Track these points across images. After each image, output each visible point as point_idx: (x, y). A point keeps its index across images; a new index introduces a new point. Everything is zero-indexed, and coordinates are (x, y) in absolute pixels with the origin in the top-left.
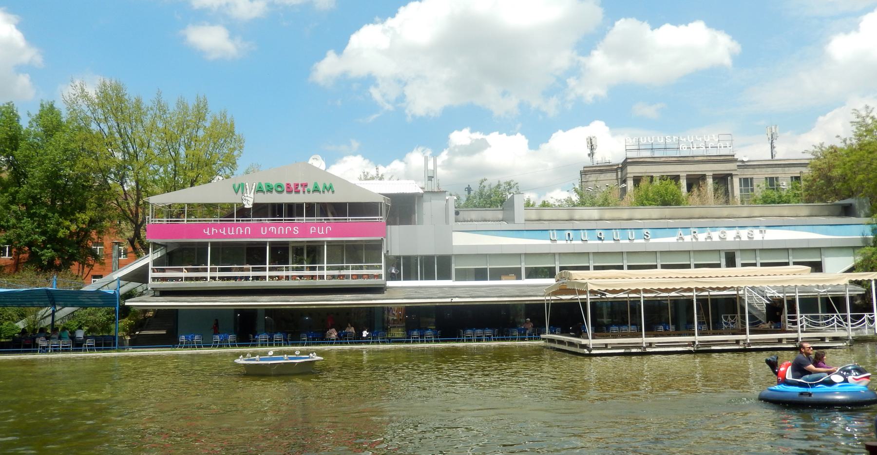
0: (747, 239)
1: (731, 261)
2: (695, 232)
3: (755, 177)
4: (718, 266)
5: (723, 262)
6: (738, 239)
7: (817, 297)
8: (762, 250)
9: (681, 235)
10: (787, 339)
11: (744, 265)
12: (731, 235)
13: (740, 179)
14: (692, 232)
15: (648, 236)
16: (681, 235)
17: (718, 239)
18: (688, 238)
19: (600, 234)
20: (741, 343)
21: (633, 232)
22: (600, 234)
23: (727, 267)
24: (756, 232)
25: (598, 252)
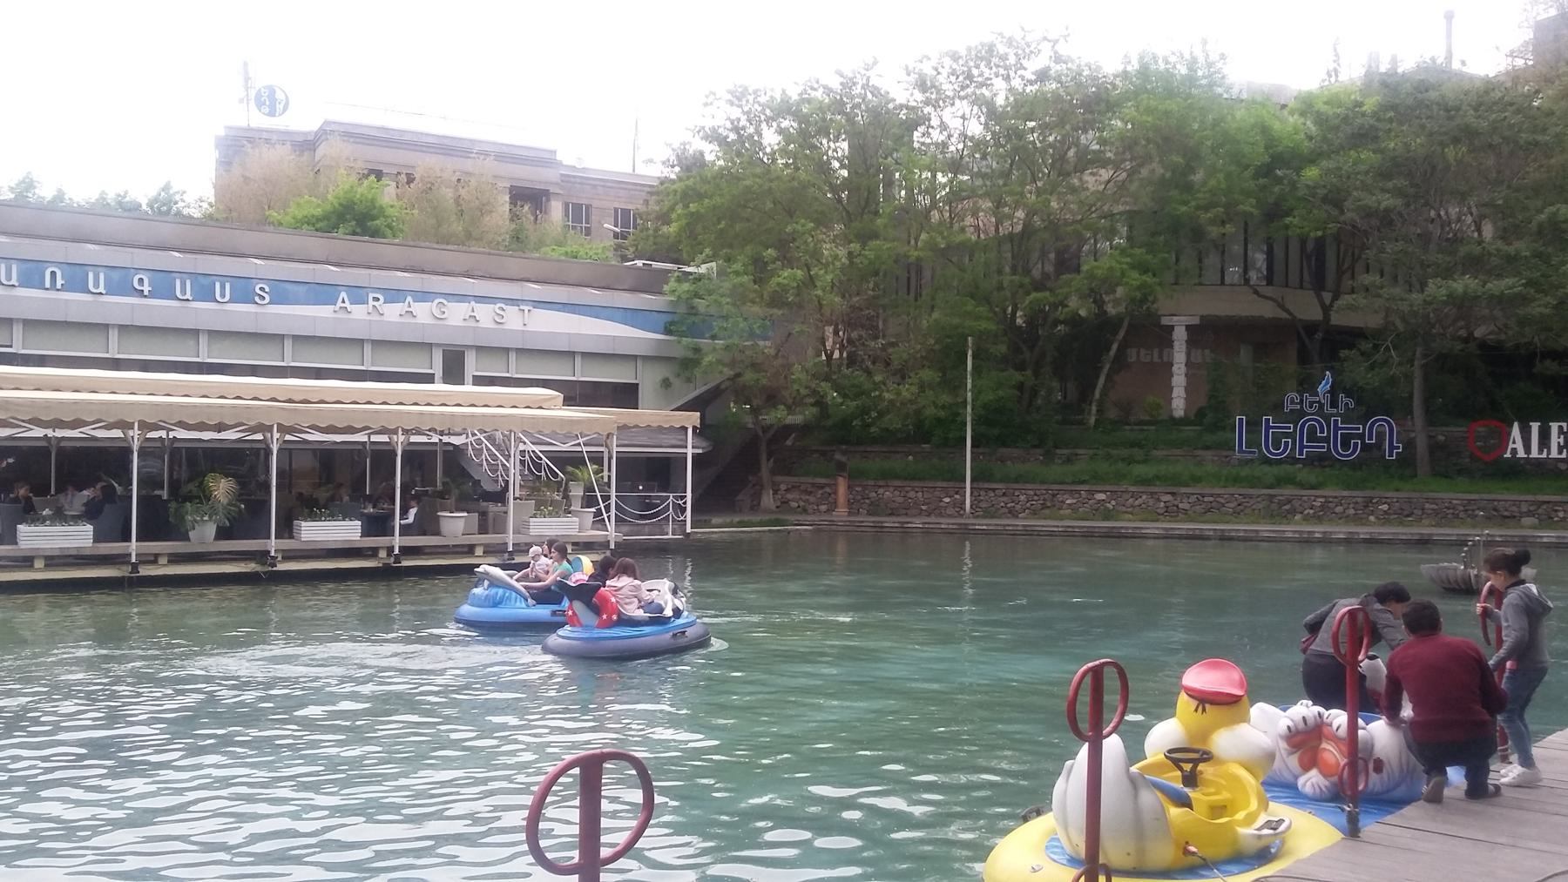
0: (494, 326)
1: (454, 370)
2: (378, 299)
3: (595, 203)
4: (429, 379)
5: (438, 370)
6: (472, 324)
7: (600, 455)
8: (520, 351)
9: (343, 302)
10: (486, 546)
11: (479, 381)
12: (457, 314)
13: (567, 205)
14: (371, 296)
15: (264, 298)
16: (343, 302)
17: (429, 321)
18: (358, 311)
19: (141, 280)
20: (383, 554)
21: (228, 286)
22: (141, 280)
23: (444, 383)
24: (512, 311)
25: (66, 323)
